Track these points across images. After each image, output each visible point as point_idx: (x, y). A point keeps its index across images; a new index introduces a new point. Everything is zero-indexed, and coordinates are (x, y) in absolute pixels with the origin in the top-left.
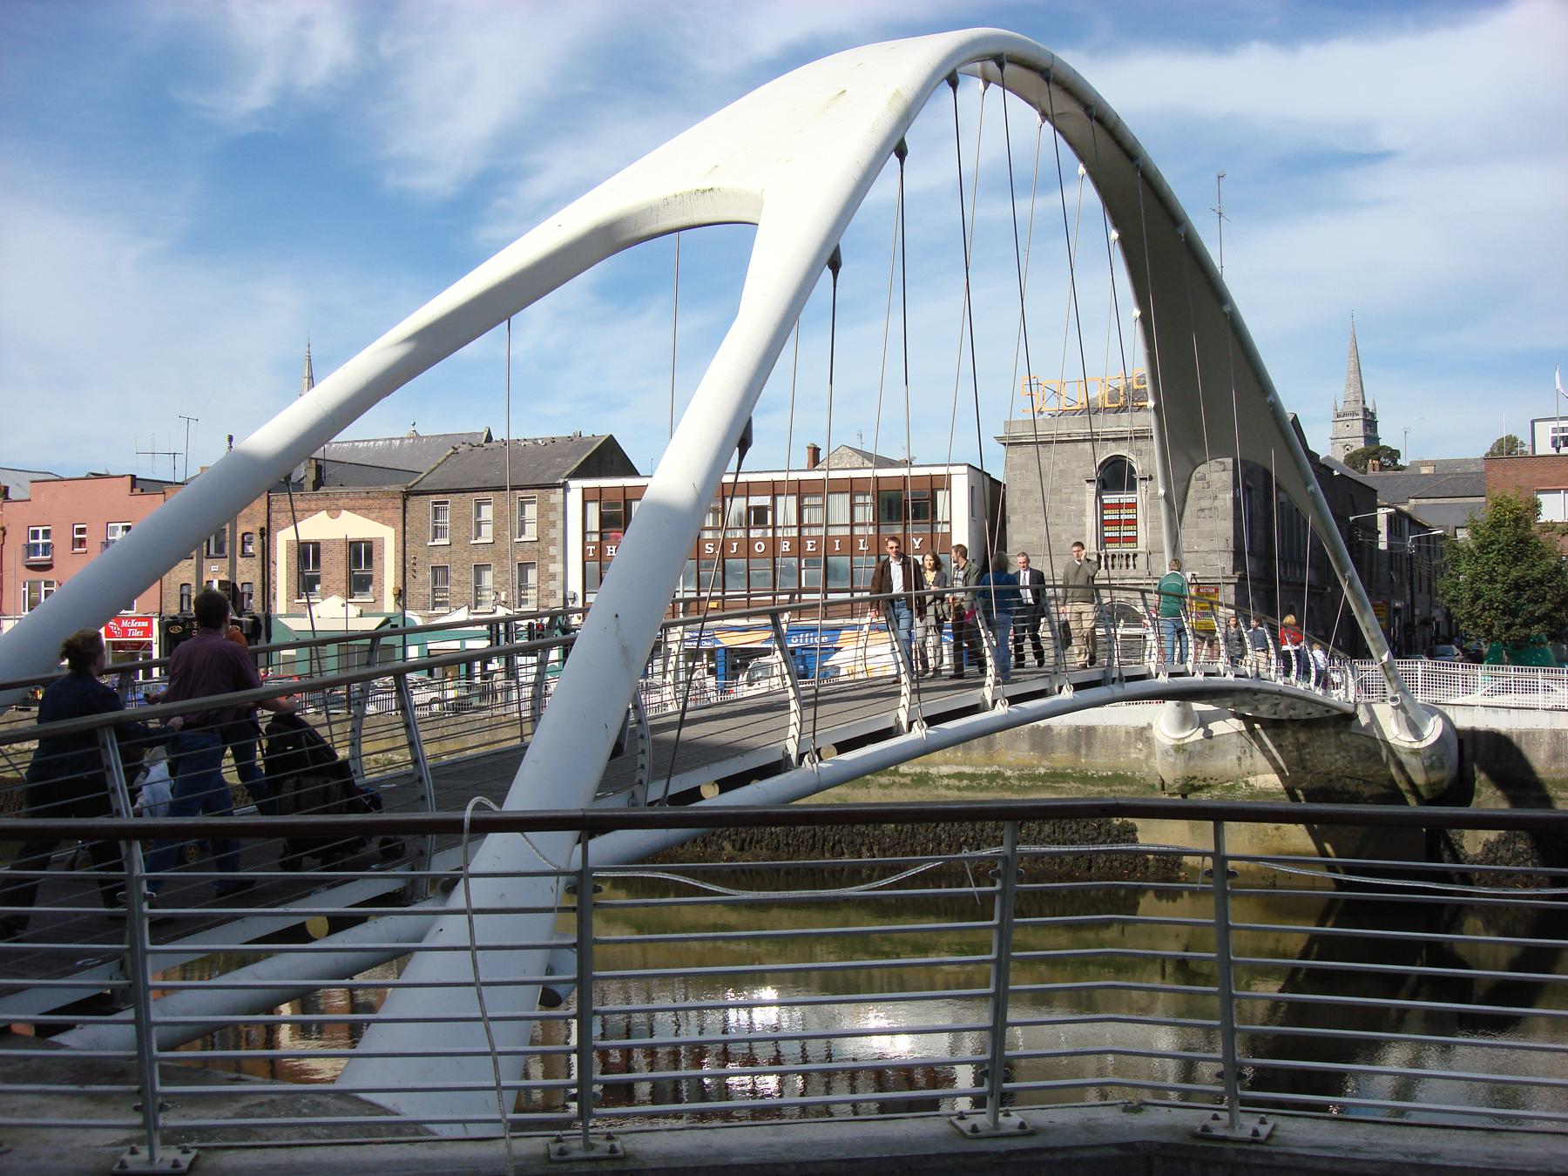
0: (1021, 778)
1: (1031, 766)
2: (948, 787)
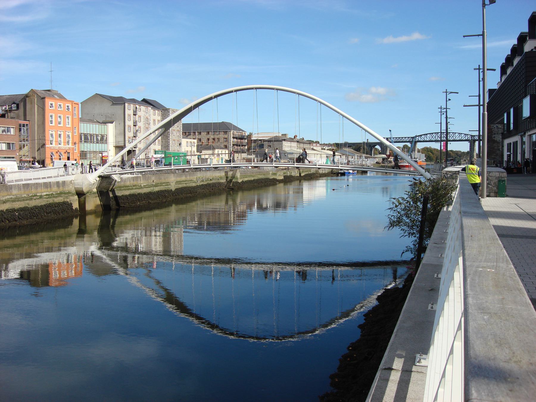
0: (56, 194)
1: (57, 191)
2: (45, 198)
